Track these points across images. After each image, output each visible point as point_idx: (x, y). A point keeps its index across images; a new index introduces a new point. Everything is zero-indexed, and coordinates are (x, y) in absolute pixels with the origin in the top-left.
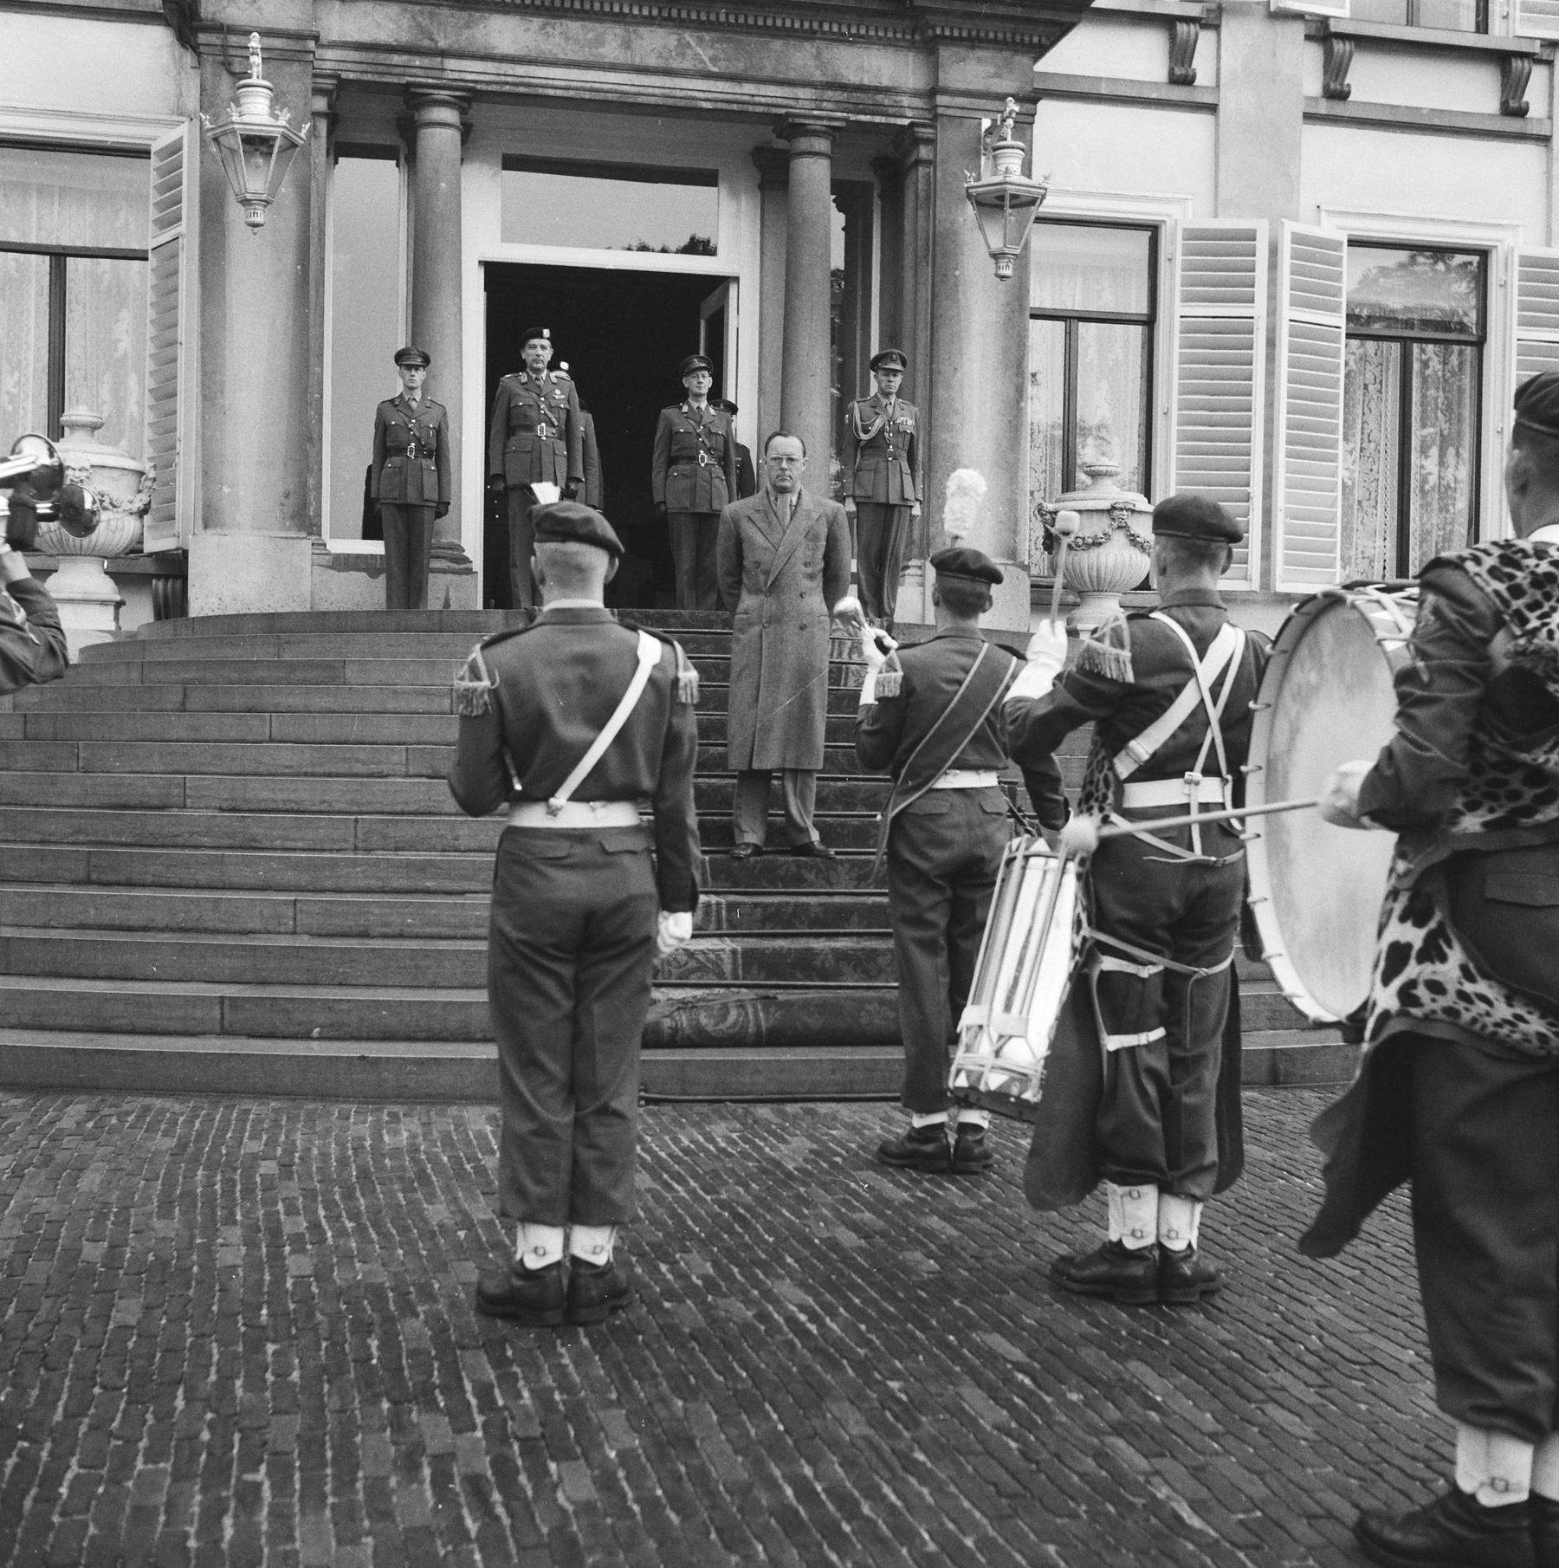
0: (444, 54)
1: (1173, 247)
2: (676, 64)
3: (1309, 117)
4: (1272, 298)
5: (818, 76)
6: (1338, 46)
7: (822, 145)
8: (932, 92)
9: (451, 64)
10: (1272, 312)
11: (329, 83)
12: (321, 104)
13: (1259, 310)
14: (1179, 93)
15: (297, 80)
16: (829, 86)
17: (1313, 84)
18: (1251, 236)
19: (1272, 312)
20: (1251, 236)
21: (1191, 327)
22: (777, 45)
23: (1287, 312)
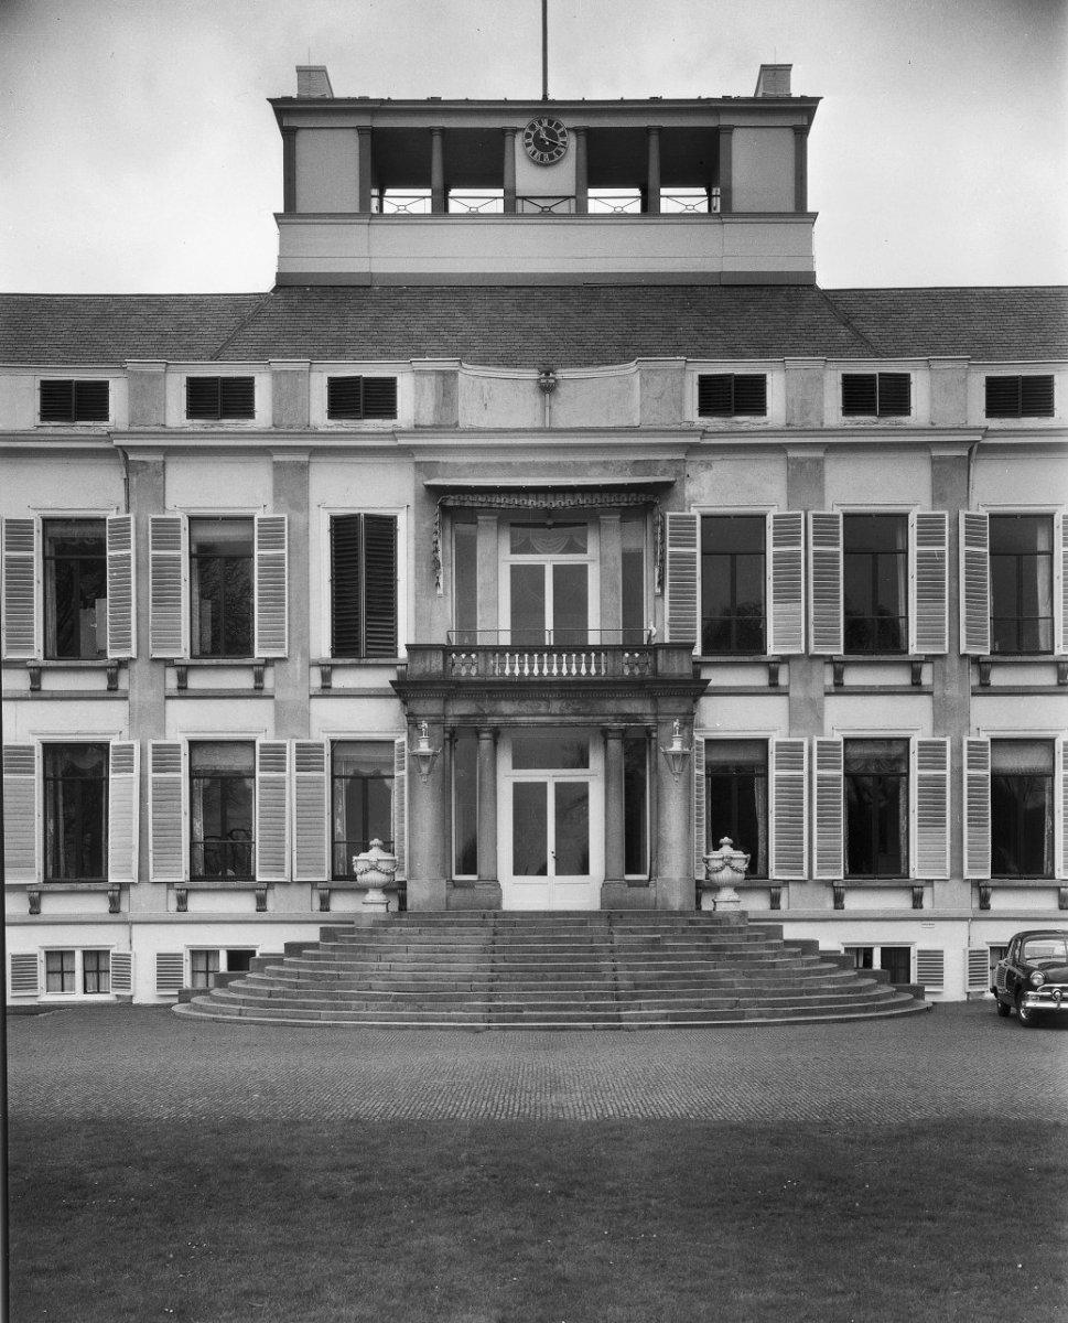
0: (489, 715)
1: (772, 747)
2: (566, 711)
3: (827, 694)
4: (810, 765)
5: (615, 711)
6: (837, 666)
7: (616, 735)
8: (656, 715)
9: (489, 719)
10: (810, 772)
11: (448, 729)
12: (447, 736)
13: (805, 772)
14: (773, 690)
15: (438, 730)
16: (620, 714)
17: (829, 681)
18: (802, 744)
19: (810, 772)
20: (802, 744)
21: (778, 779)
22: (602, 702)
23: (816, 772)
